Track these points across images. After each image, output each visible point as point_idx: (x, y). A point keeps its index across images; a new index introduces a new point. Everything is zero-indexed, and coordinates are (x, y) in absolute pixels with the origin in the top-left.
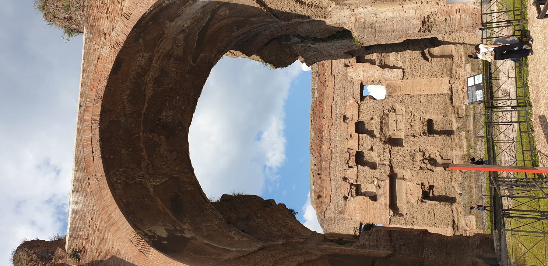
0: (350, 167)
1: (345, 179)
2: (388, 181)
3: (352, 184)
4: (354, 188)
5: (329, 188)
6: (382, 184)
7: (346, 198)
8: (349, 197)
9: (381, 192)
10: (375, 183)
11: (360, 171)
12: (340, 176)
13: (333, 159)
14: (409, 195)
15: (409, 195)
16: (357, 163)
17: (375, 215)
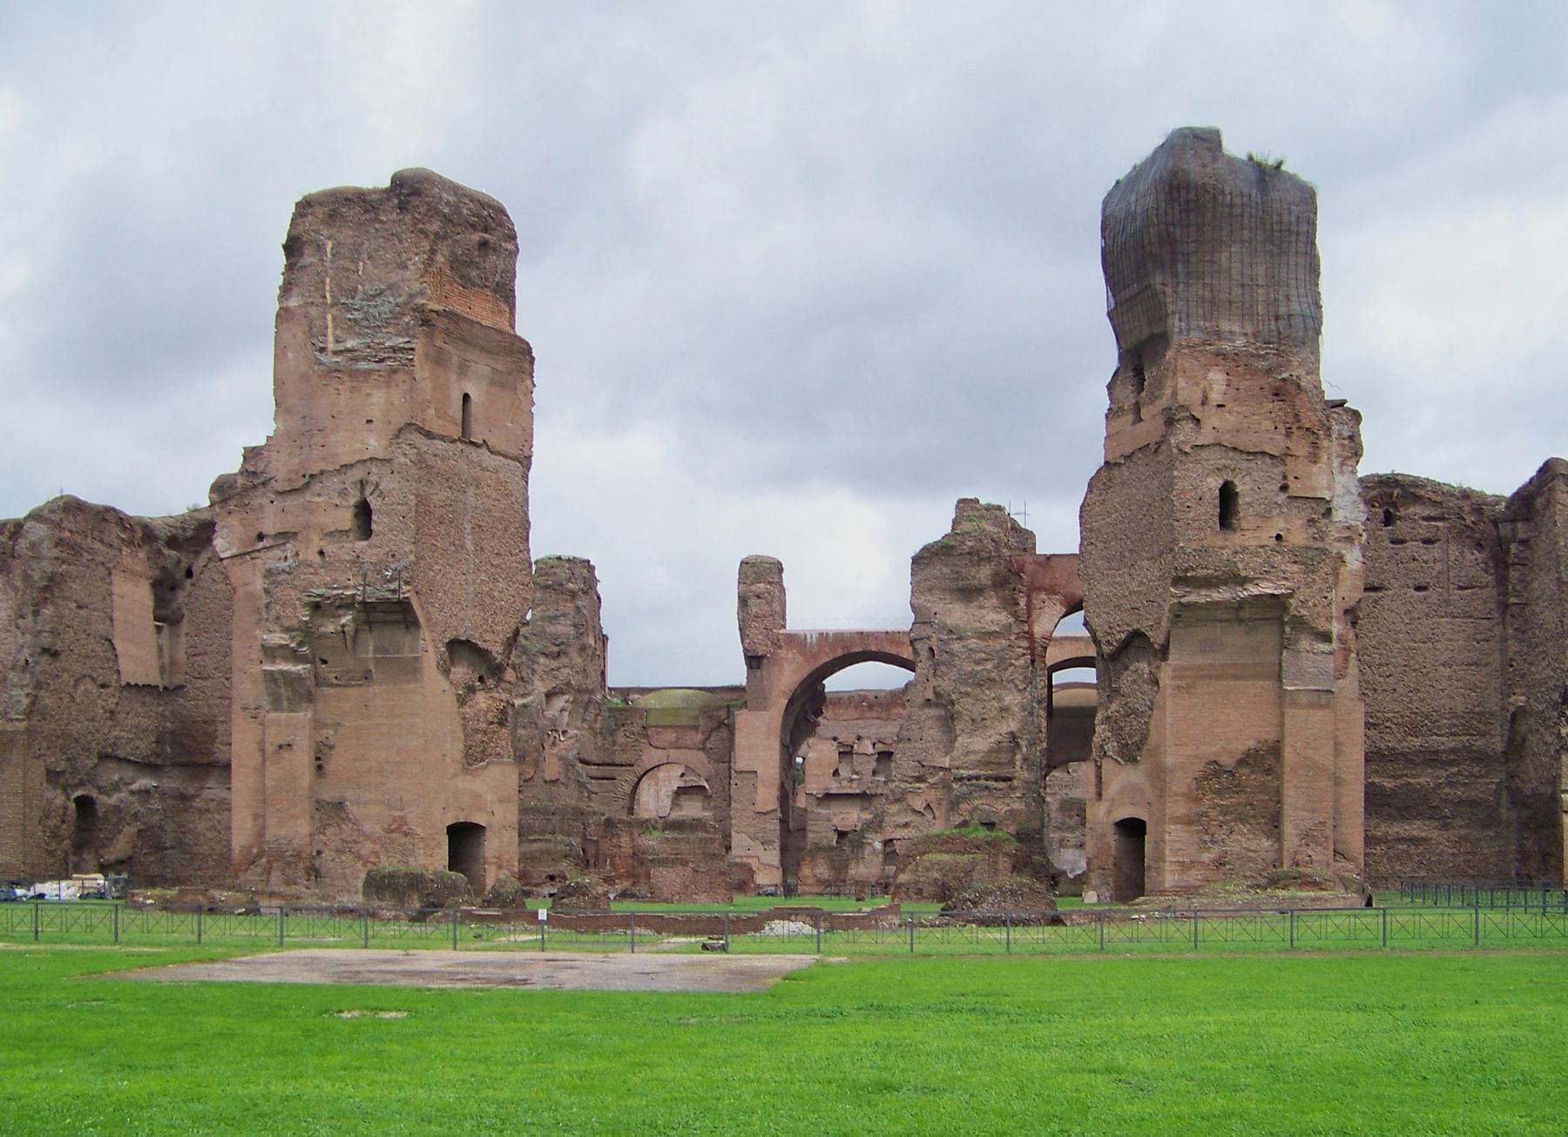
0: (874, 745)
1: (859, 738)
2: (857, 791)
3: (852, 747)
4: (849, 749)
5: (845, 717)
6: (855, 785)
7: (835, 739)
8: (835, 743)
9: (845, 783)
10: (854, 776)
11: (868, 758)
12: (862, 732)
13: (883, 723)
14: (841, 816)
15: (841, 816)
16: (879, 753)
17: (816, 775)
